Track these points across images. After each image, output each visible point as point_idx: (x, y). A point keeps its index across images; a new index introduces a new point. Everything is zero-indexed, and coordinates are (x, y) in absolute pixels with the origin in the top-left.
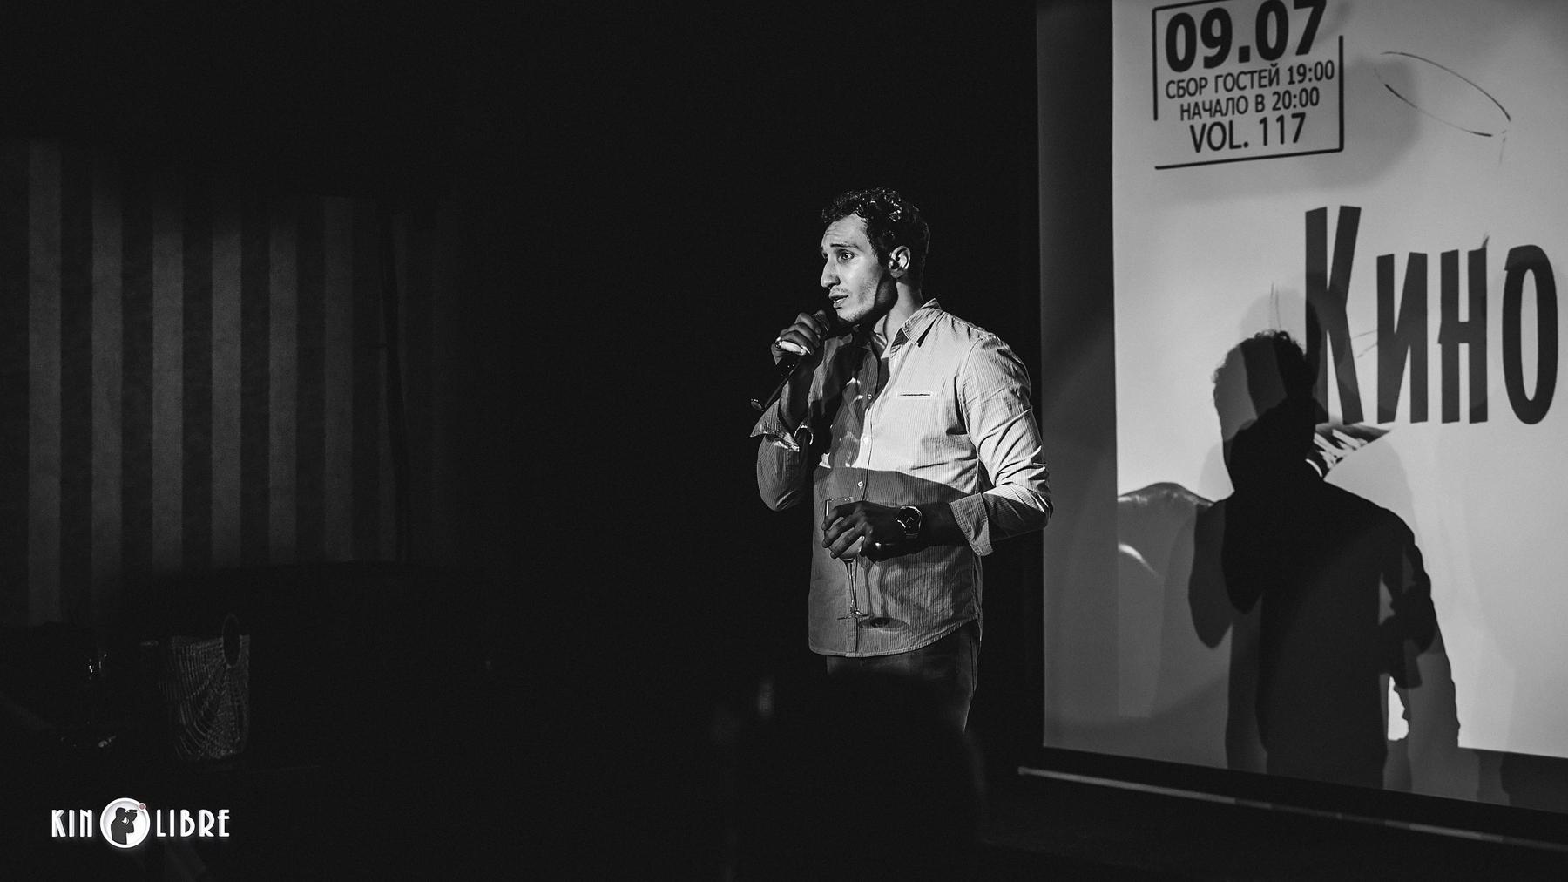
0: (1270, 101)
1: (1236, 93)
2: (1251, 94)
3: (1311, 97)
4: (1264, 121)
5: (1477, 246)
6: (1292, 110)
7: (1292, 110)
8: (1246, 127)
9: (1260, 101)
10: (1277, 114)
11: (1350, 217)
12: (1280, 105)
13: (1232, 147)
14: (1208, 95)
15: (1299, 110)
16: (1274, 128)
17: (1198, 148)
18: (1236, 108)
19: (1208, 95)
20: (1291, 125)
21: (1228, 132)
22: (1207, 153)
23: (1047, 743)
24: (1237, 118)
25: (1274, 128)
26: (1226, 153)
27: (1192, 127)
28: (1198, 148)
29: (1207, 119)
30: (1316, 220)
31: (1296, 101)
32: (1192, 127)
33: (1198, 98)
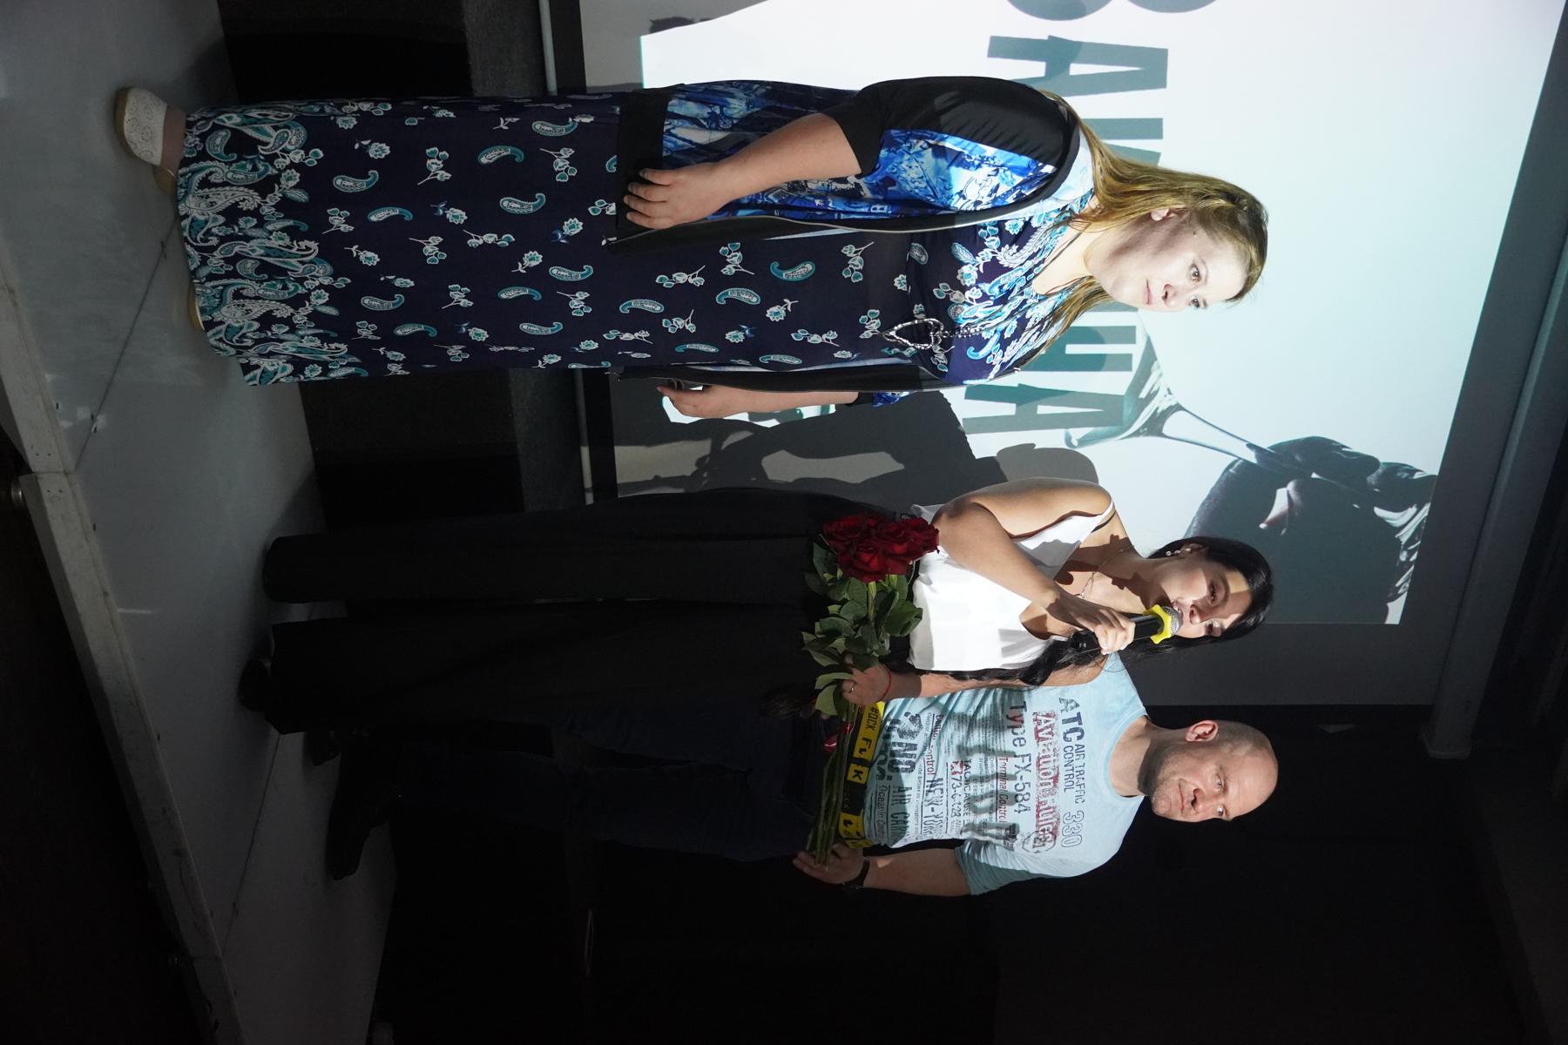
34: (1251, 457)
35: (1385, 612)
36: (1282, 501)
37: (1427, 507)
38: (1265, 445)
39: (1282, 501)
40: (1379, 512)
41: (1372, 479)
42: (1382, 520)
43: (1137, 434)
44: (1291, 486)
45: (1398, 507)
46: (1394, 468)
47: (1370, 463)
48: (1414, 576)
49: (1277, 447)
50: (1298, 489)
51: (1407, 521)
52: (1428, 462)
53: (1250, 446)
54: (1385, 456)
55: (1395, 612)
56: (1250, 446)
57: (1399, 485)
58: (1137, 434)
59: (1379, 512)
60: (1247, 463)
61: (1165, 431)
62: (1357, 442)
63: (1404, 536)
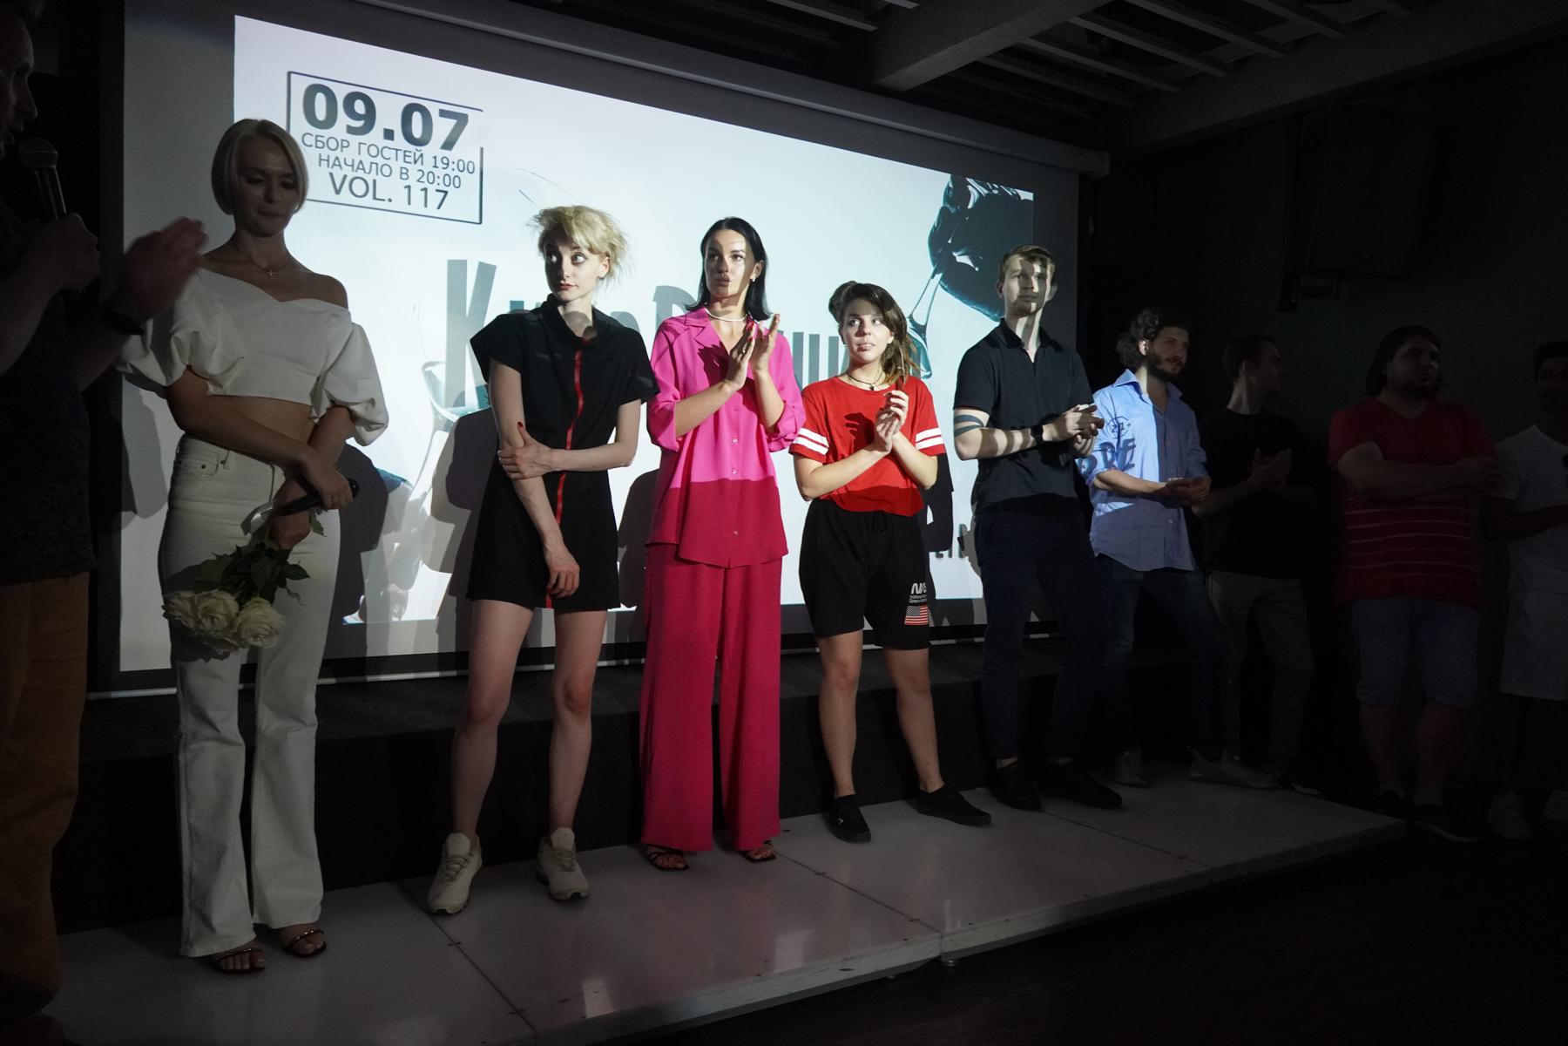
0: (413, 170)
1: (380, 160)
3: (455, 182)
6: (435, 186)
7: (435, 186)
8: (390, 187)
9: (404, 173)
11: (486, 273)
14: (350, 154)
17: (338, 192)
18: (379, 170)
19: (350, 154)
20: (435, 198)
21: (372, 189)
22: (345, 195)
23: (127, 664)
24: (379, 178)
28: (338, 192)
29: (347, 170)
30: (456, 269)
33: (338, 153)
34: (939, 276)
35: (1026, 201)
37: (970, 181)
41: (953, 210)
42: (975, 204)
45: (968, 195)
46: (947, 198)
47: (943, 211)
48: (1009, 185)
49: (934, 262)
51: (975, 190)
52: (943, 180)
54: (939, 203)
55: (1026, 195)
57: (956, 195)
62: (932, 219)
63: (984, 191)
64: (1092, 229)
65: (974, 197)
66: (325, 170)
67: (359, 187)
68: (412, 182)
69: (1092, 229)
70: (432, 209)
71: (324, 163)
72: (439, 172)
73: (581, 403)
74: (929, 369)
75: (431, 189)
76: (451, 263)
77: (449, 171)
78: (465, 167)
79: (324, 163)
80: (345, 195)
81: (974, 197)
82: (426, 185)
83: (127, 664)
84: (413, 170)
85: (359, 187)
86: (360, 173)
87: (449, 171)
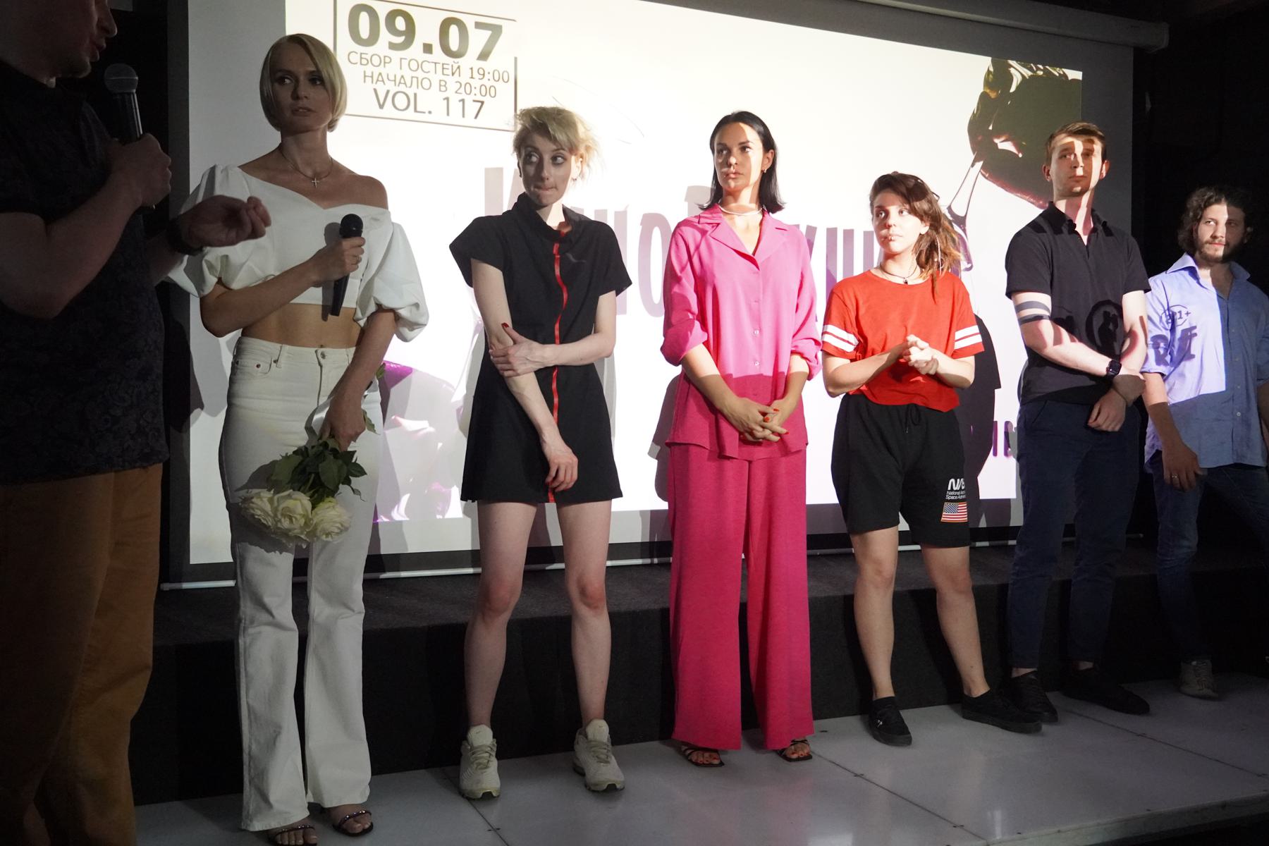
0: (452, 82)
2: (436, 78)
3: (489, 91)
4: (447, 99)
5: (621, 209)
6: (472, 97)
7: (472, 97)
8: (430, 100)
9: (443, 86)
10: (461, 97)
12: (462, 90)
13: (416, 110)
15: (482, 99)
16: (456, 107)
17: (381, 106)
18: (420, 83)
20: (472, 108)
21: (412, 102)
22: (389, 110)
23: (196, 558)
24: (420, 92)
25: (456, 107)
26: (410, 113)
27: (375, 90)
28: (381, 106)
31: (477, 91)
32: (375, 90)
34: (979, 165)
36: (1006, 145)
38: (972, 157)
39: (1006, 145)
40: (1013, 89)
41: (993, 95)
42: (1018, 87)
43: (964, 231)
44: (996, 141)
45: (1010, 78)
46: (987, 83)
47: (983, 97)
49: (974, 150)
50: (998, 137)
53: (973, 165)
54: (980, 89)
56: (973, 165)
57: (997, 79)
58: (964, 231)
59: (1013, 89)
60: (983, 167)
61: (962, 214)
62: (971, 105)
64: (1148, 106)
65: (1017, 80)
66: (369, 86)
67: (401, 101)
68: (450, 93)
69: (1148, 106)
70: (469, 119)
71: (369, 80)
72: (476, 83)
73: (565, 296)
74: (969, 260)
75: (469, 99)
76: (487, 170)
77: (485, 81)
78: (501, 78)
79: (369, 80)
80: (389, 110)
81: (1017, 80)
82: (463, 96)
83: (196, 558)
84: (452, 82)
85: (401, 101)
86: (402, 88)
87: (485, 81)
